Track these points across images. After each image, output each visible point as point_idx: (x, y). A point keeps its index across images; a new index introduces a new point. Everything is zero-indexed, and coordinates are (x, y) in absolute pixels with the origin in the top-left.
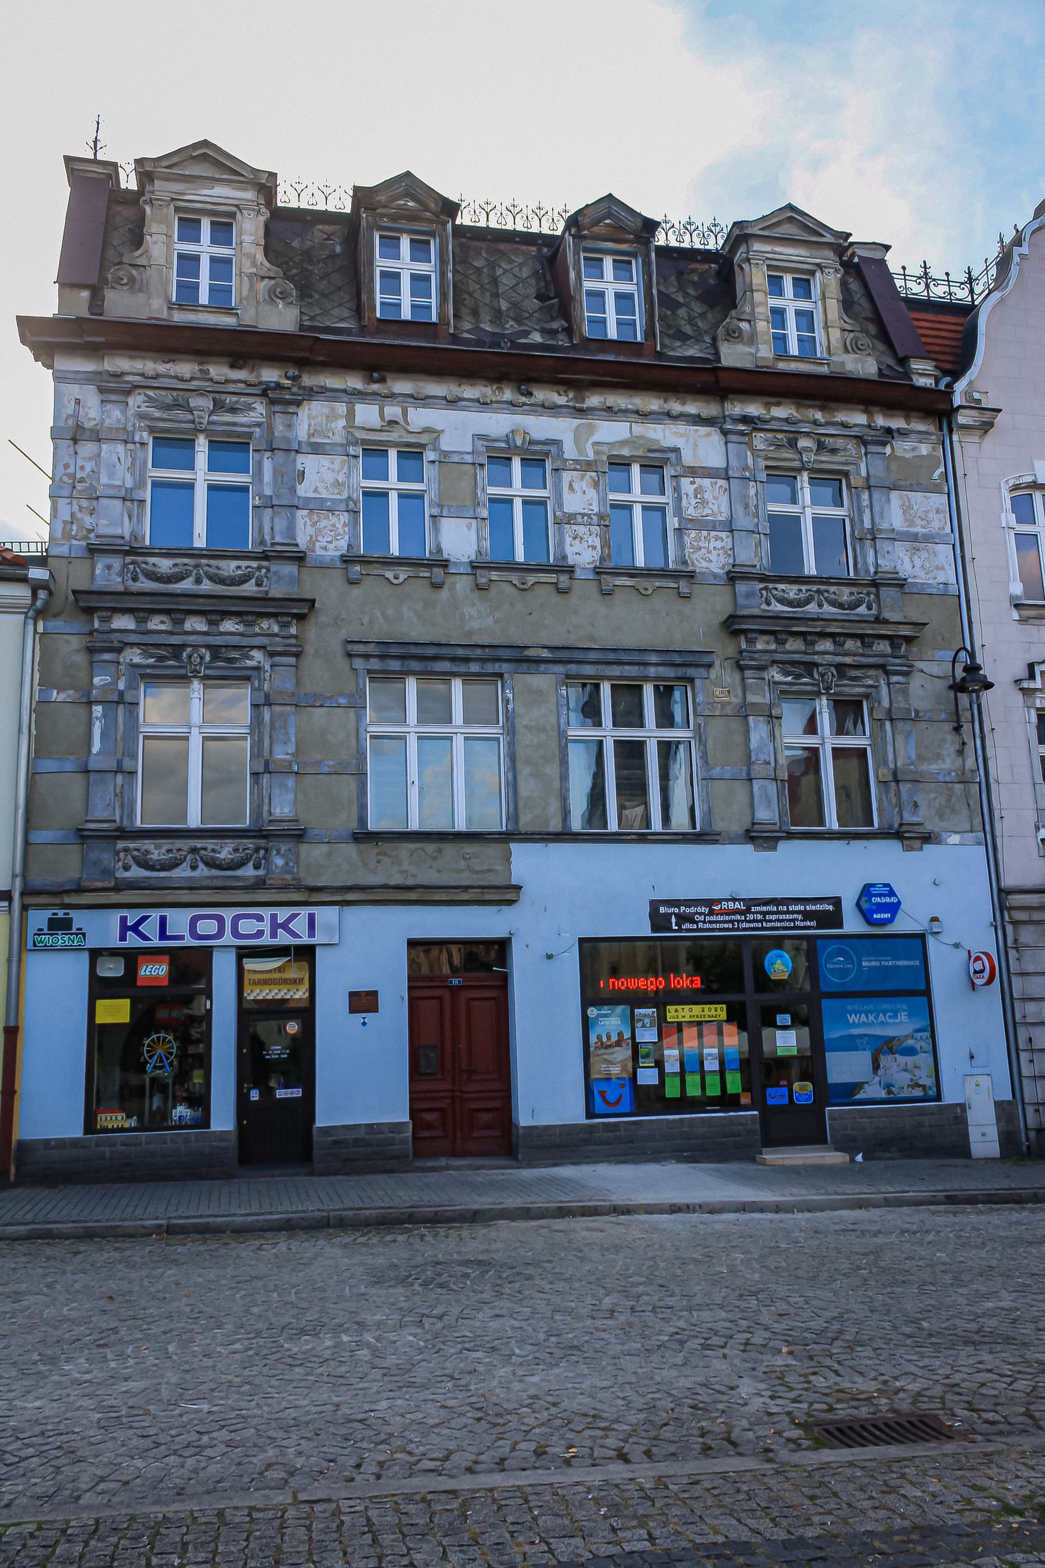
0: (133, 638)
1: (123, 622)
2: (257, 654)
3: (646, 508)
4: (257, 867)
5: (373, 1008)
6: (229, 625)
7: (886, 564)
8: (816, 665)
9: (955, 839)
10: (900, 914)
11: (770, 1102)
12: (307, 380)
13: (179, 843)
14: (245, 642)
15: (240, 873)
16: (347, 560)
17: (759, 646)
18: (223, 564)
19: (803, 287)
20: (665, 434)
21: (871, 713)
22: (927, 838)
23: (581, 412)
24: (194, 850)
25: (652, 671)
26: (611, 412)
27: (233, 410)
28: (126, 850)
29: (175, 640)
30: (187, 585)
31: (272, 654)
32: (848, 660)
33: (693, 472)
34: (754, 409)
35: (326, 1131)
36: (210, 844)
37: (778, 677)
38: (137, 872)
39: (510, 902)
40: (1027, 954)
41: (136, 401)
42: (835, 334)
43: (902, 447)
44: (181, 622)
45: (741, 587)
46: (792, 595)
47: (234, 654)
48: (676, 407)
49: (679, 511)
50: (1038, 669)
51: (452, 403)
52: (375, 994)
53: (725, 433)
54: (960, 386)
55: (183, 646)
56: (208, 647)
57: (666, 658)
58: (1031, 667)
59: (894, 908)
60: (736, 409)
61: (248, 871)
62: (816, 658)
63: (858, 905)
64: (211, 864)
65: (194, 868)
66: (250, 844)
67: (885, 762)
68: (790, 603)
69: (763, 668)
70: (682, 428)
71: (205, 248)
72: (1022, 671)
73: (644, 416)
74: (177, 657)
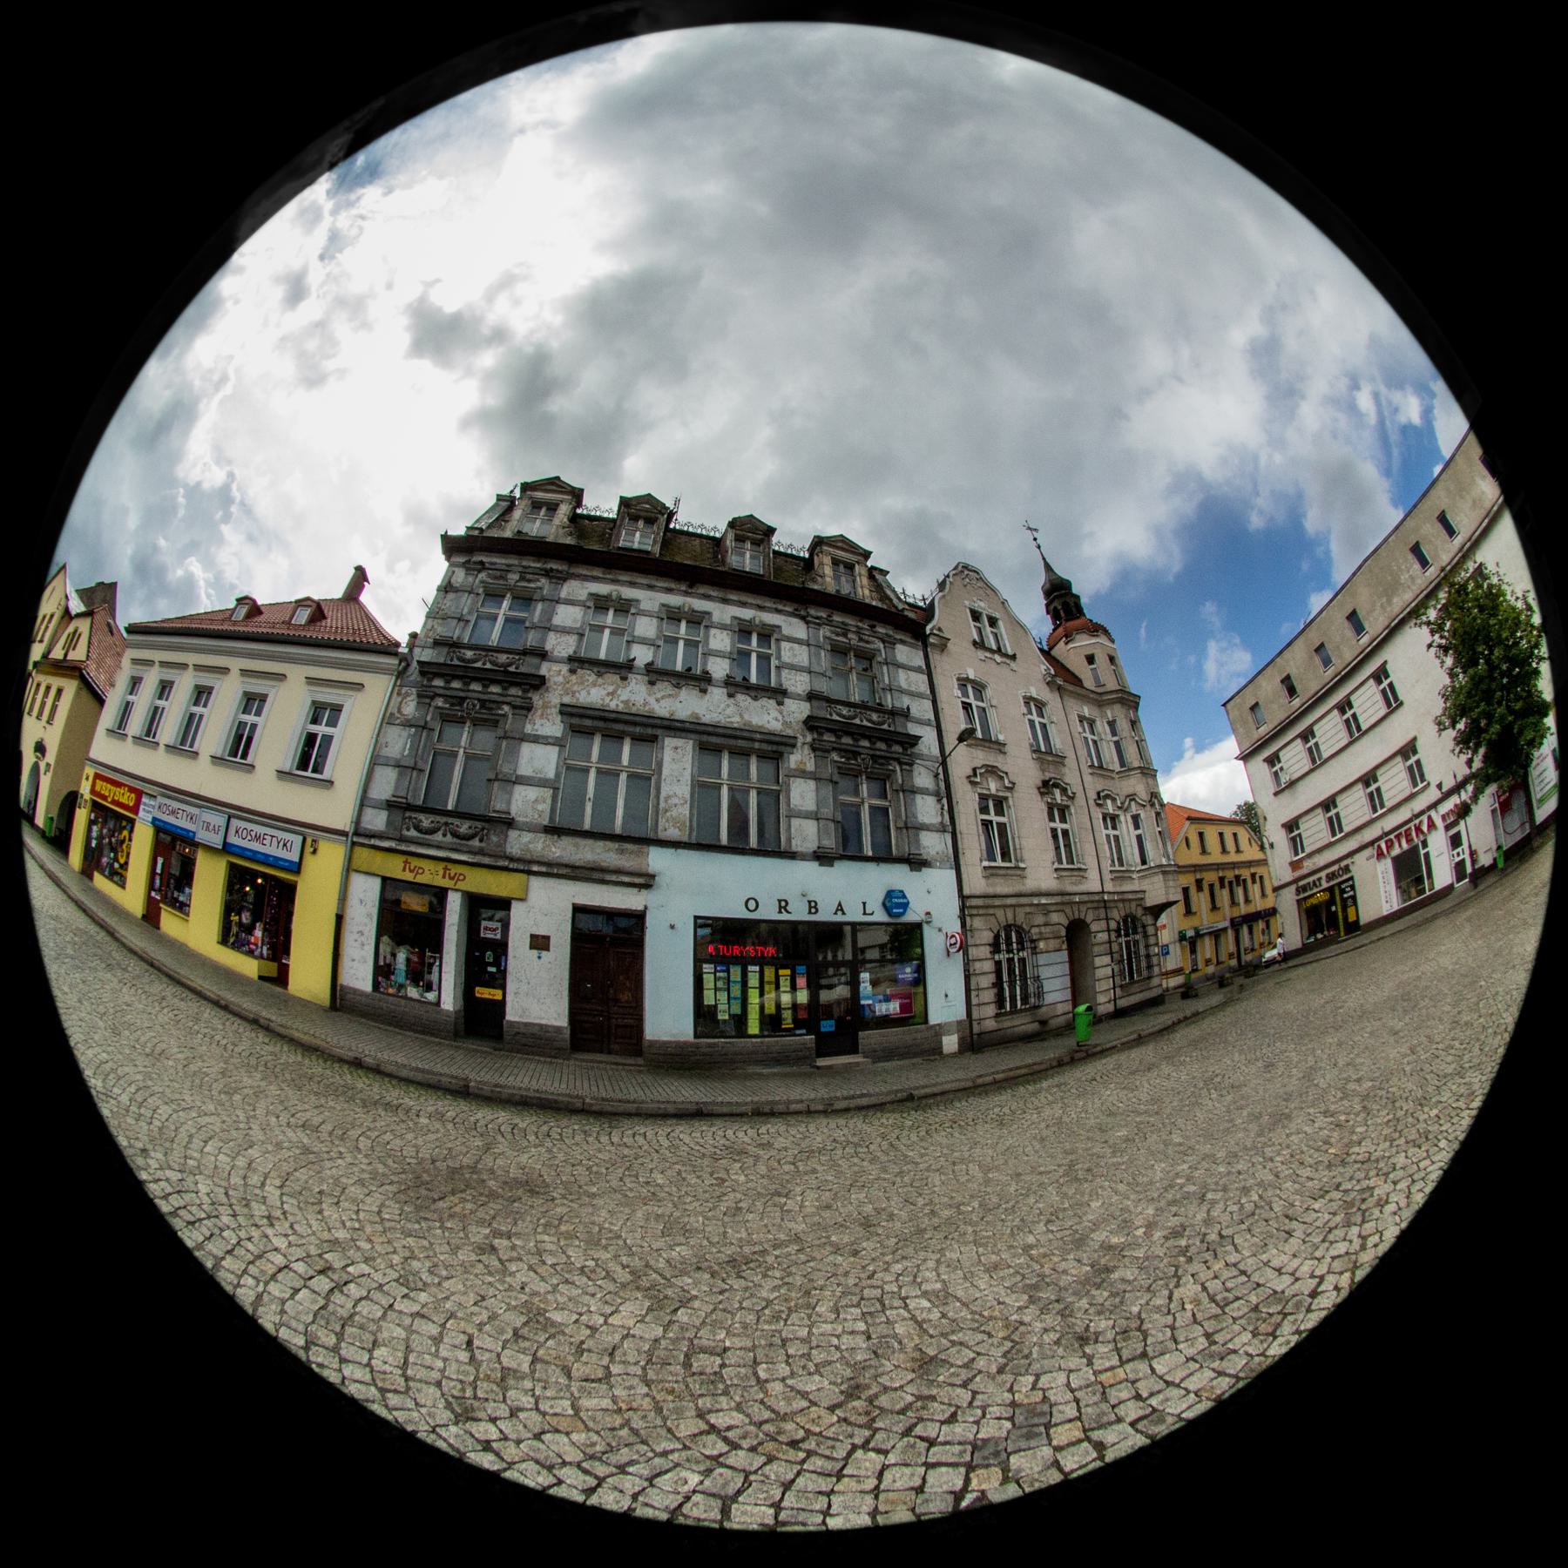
0: (441, 691)
1: (438, 682)
2: (506, 708)
3: (760, 656)
4: (481, 841)
5: (547, 949)
6: (495, 689)
7: (897, 704)
8: (860, 754)
10: (909, 911)
11: (823, 1030)
12: (572, 571)
13: (438, 818)
14: (501, 699)
15: (470, 843)
16: (571, 659)
17: (825, 738)
18: (499, 655)
21: (891, 786)
24: (446, 824)
25: (757, 745)
27: (529, 581)
28: (410, 818)
29: (462, 694)
31: (514, 707)
32: (878, 753)
35: (511, 1023)
36: (456, 821)
37: (836, 758)
38: (413, 833)
39: (648, 886)
40: (977, 934)
41: (482, 576)
44: (469, 684)
46: (844, 712)
47: (494, 706)
48: (780, 607)
49: (779, 657)
50: (978, 771)
51: (651, 587)
52: (547, 938)
53: (807, 623)
55: (466, 698)
56: (479, 700)
57: (767, 737)
58: (974, 770)
59: (905, 906)
61: (476, 843)
62: (860, 750)
63: (884, 904)
64: (455, 835)
65: (444, 835)
66: (479, 825)
67: (900, 816)
68: (844, 717)
69: (828, 751)
70: (783, 617)
72: (970, 772)
73: (760, 608)
74: (461, 704)
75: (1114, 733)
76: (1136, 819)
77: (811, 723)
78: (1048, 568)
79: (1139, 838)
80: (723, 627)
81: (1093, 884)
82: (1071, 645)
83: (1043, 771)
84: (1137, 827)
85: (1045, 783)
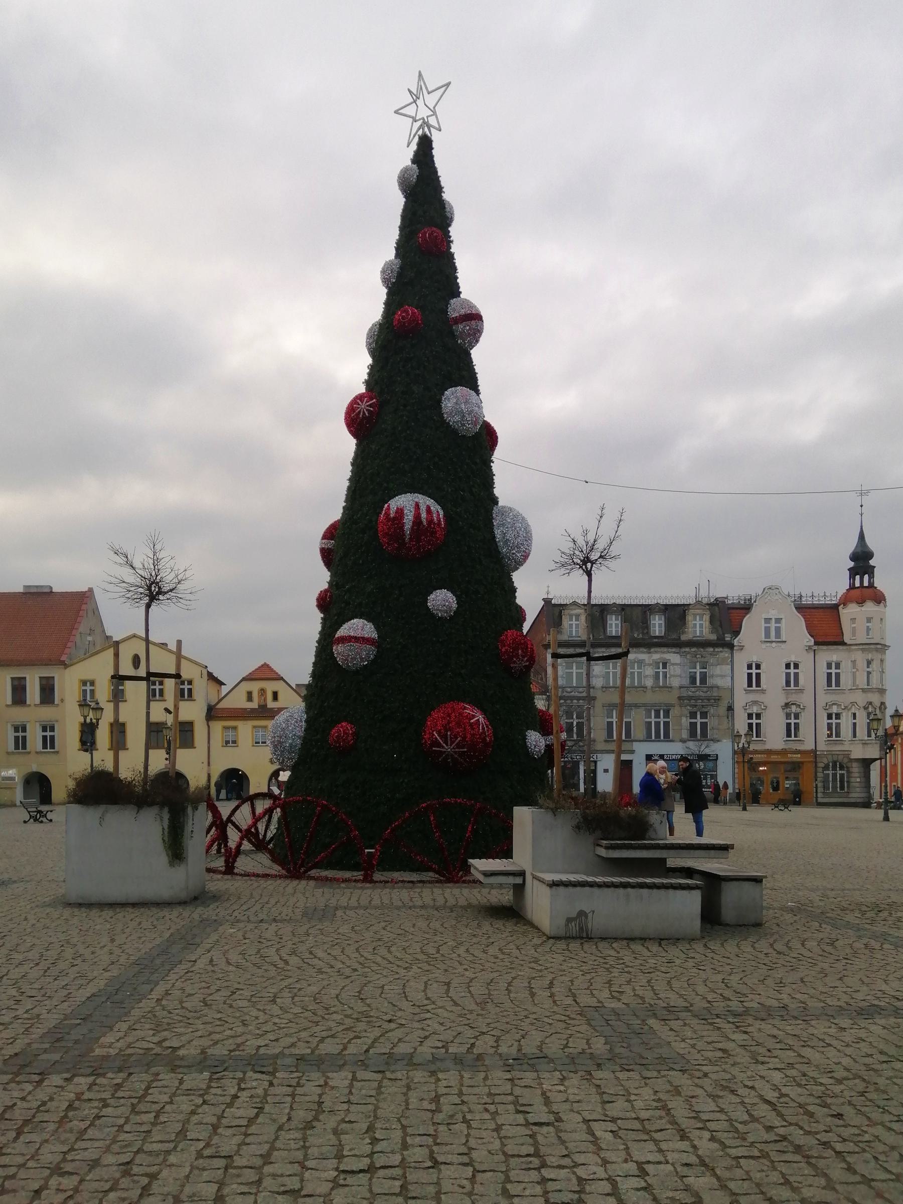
6: (581, 701)
7: (715, 682)
9: (725, 741)
16: (602, 687)
19: (701, 619)
20: (667, 656)
22: (718, 741)
23: (650, 653)
26: (656, 652)
30: (573, 693)
33: (673, 664)
34: (687, 649)
42: (707, 630)
43: (721, 655)
45: (682, 689)
54: (736, 641)
60: (683, 650)
70: (672, 654)
71: (574, 622)
73: (664, 653)
75: (854, 667)
76: (854, 715)
77: (680, 698)
78: (862, 536)
79: (855, 724)
80: (650, 665)
81: (809, 746)
82: (845, 611)
83: (787, 699)
84: (855, 718)
85: (787, 705)
